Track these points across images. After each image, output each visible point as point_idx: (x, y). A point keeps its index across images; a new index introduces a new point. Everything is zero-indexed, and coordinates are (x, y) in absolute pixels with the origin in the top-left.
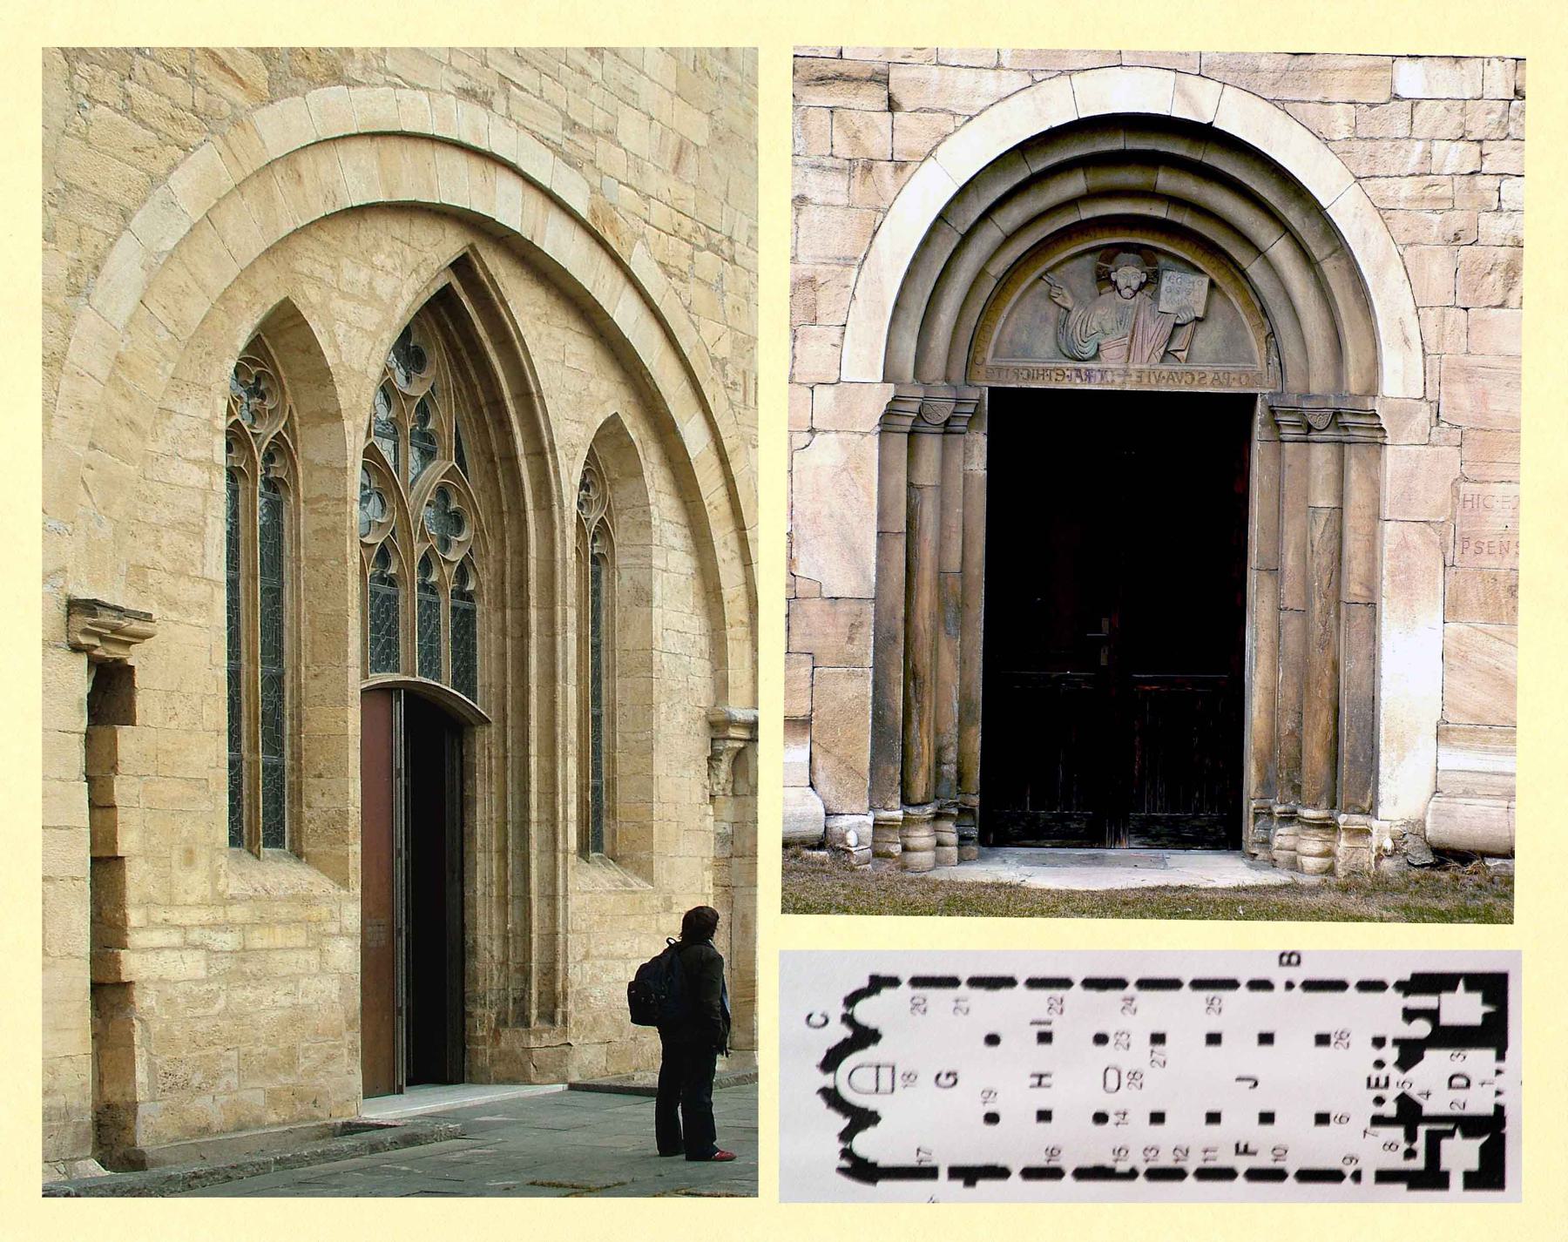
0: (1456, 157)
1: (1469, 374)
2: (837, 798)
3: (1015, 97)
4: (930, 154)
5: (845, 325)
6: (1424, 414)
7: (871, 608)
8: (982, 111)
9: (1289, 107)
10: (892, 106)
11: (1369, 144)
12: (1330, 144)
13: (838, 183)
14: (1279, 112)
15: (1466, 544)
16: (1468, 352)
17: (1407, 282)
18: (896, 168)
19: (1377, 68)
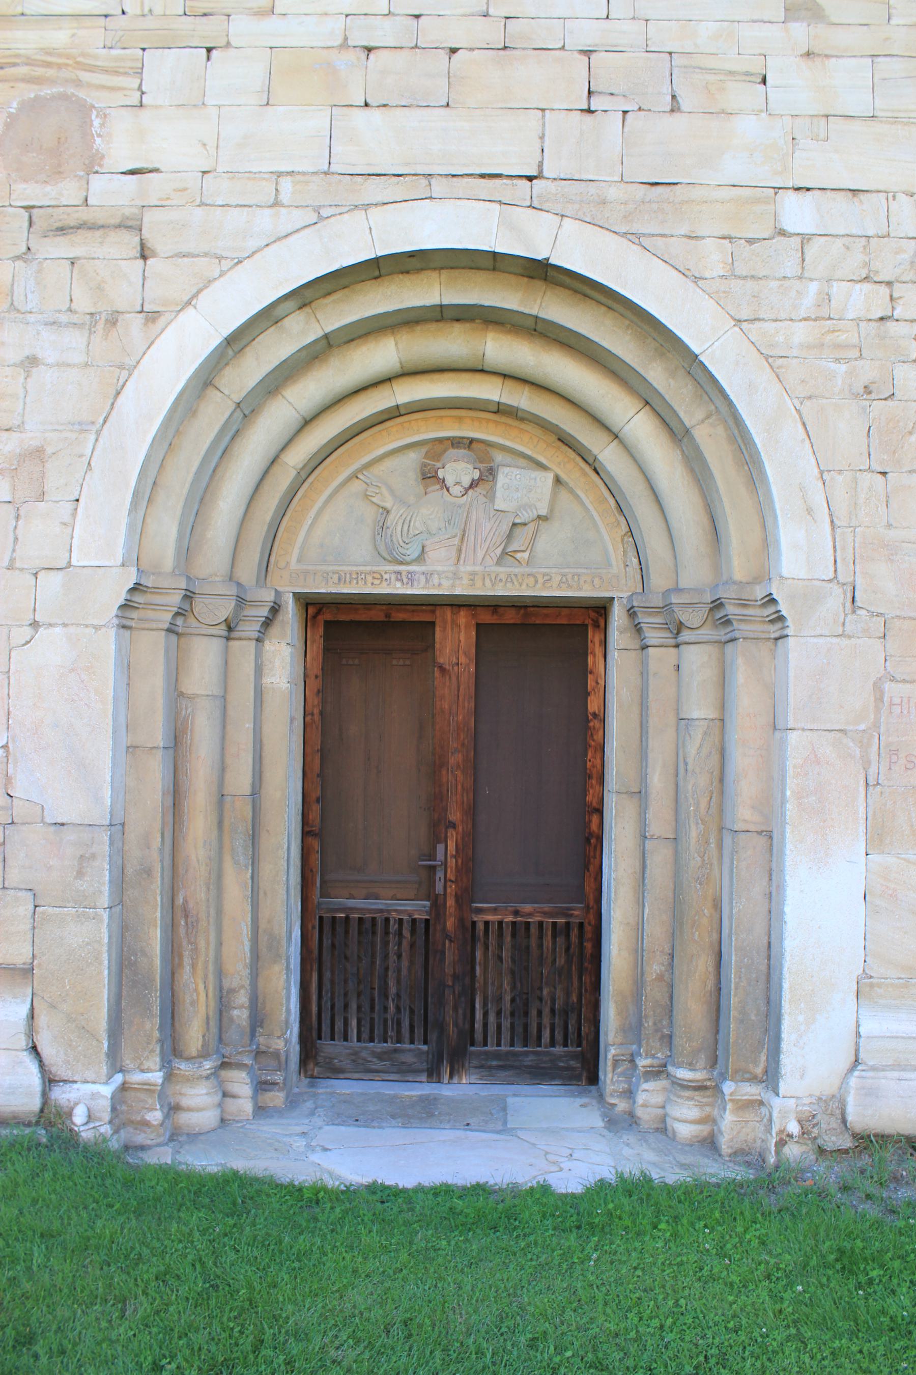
2: (67, 1062)
3: (296, 236)
4: (189, 303)
5: (77, 500)
6: (836, 599)
7: (105, 837)
8: (254, 253)
9: (645, 241)
11: (750, 284)
12: (700, 283)
13: (75, 340)
14: (635, 247)
15: (894, 758)
16: (889, 526)
17: (807, 441)
18: (147, 320)
19: (757, 201)
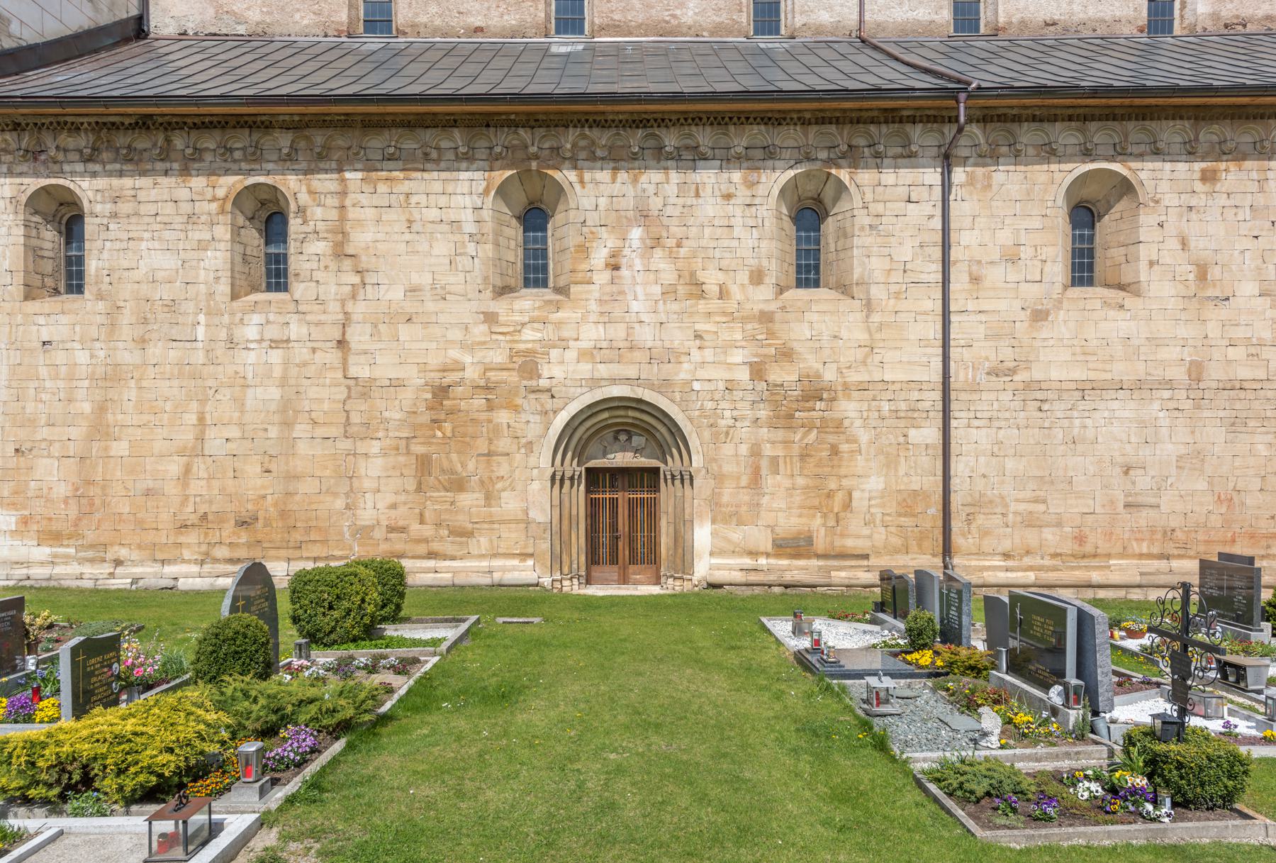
0: (709, 405)
1: (715, 460)
6: (704, 471)
10: (553, 397)
